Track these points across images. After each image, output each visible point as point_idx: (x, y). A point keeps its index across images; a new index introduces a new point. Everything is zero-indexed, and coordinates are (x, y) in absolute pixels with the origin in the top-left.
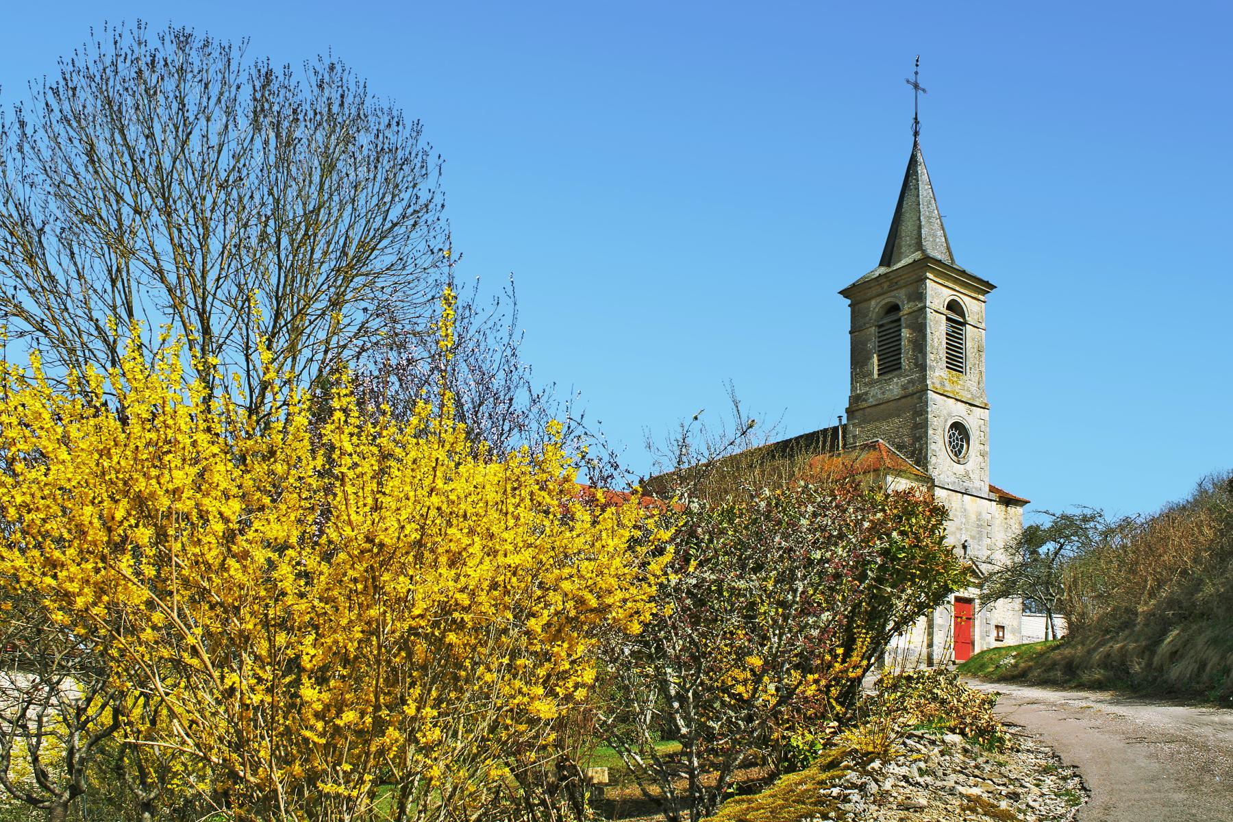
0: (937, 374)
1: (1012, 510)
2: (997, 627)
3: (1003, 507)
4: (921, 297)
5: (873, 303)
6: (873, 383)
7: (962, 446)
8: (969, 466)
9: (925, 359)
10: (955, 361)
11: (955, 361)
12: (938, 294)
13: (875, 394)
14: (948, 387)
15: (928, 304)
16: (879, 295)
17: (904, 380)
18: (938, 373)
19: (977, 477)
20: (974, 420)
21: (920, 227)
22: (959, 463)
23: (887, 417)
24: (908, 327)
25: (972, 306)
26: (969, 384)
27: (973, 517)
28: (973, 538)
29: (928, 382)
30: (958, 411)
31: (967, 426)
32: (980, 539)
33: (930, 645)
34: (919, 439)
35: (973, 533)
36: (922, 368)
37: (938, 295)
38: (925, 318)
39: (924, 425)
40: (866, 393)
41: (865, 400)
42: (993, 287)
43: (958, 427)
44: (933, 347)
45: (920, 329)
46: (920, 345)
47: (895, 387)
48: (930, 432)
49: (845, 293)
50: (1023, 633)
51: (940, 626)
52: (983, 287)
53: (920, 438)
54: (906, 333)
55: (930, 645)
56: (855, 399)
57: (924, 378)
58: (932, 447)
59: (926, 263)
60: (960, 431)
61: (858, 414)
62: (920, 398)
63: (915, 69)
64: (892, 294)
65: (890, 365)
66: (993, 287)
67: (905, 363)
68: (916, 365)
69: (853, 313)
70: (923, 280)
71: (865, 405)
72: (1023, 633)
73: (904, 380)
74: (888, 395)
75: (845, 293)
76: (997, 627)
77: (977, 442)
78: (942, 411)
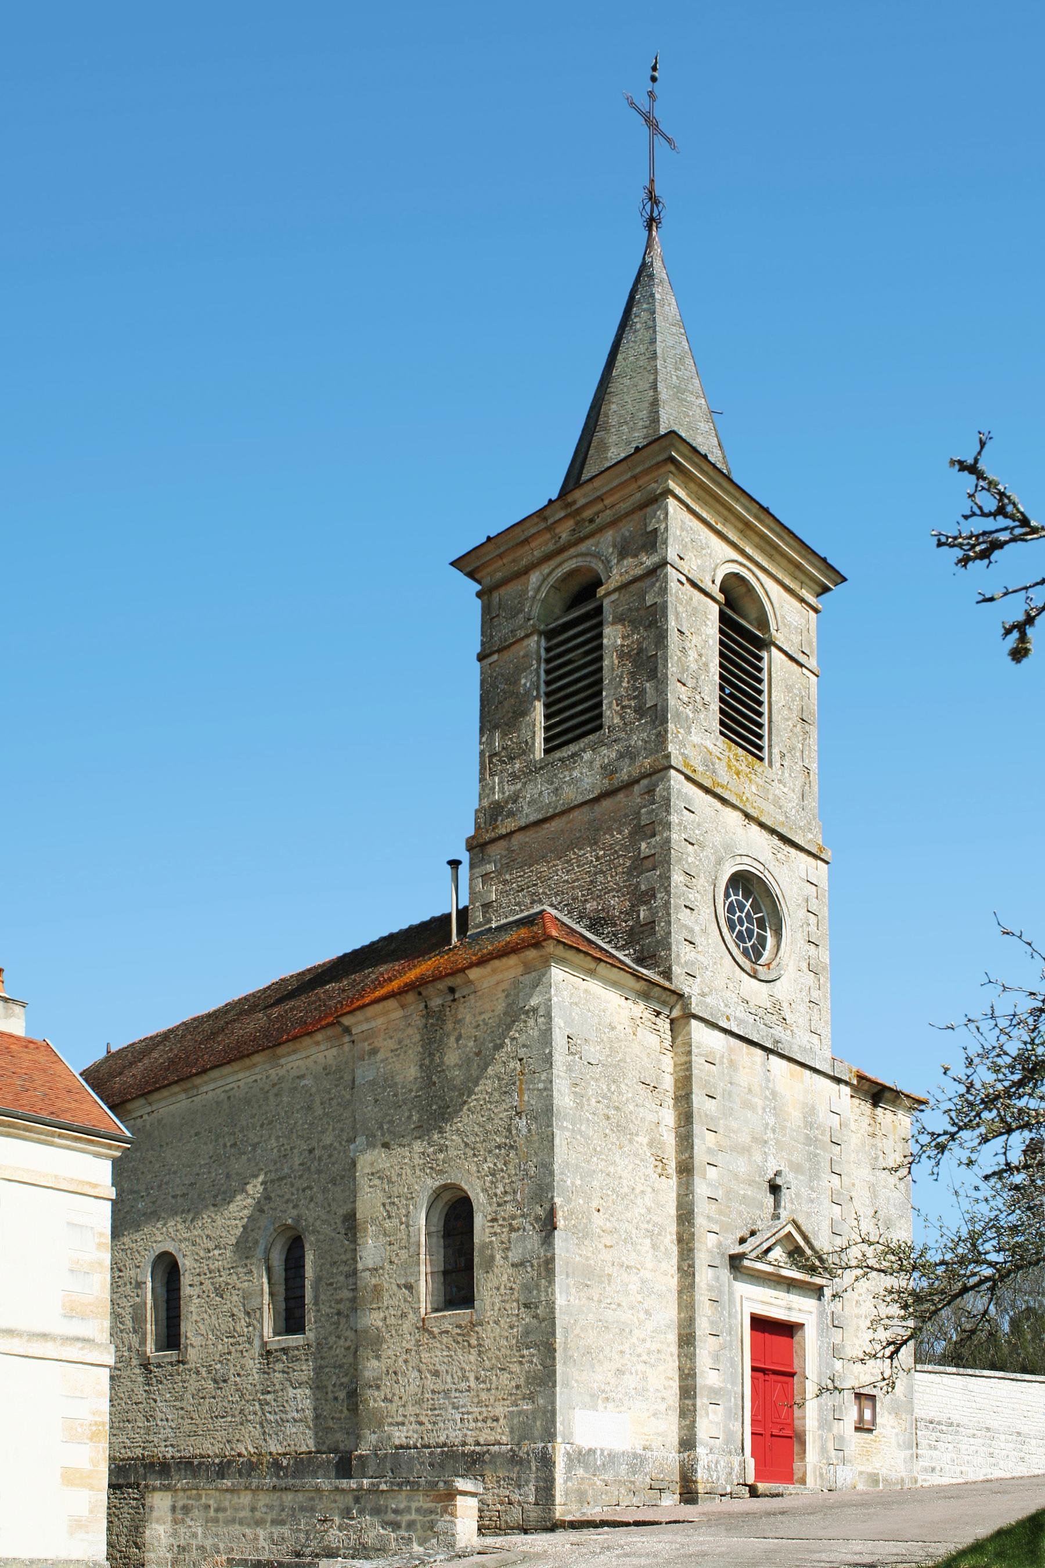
0: (695, 738)
1: (885, 1115)
2: (858, 1396)
3: (866, 1107)
4: (652, 540)
5: (534, 578)
6: (534, 770)
7: (762, 941)
8: (783, 989)
9: (661, 690)
10: (742, 718)
11: (742, 718)
12: (697, 550)
13: (537, 795)
14: (724, 776)
15: (672, 555)
16: (547, 558)
17: (609, 754)
18: (695, 734)
19: (802, 1021)
20: (791, 878)
21: (655, 403)
22: (754, 976)
23: (560, 850)
24: (619, 620)
25: (787, 615)
26: (786, 780)
27: (795, 1116)
28: (797, 1168)
29: (671, 748)
30: (756, 850)
31: (776, 890)
32: (814, 1176)
33: (688, 1443)
34: (647, 897)
35: (796, 1157)
36: (656, 716)
37: (701, 549)
38: (664, 591)
39: (660, 861)
40: (515, 798)
41: (511, 814)
42: (845, 579)
43: (745, 883)
44: (685, 669)
45: (651, 620)
46: (649, 664)
47: (586, 772)
48: (677, 878)
49: (468, 564)
50: (919, 1413)
51: (714, 1391)
52: (820, 576)
53: (650, 895)
54: (613, 636)
55: (688, 1443)
56: (491, 814)
57: (662, 738)
58: (681, 917)
59: (665, 453)
60: (752, 903)
61: (496, 851)
62: (650, 791)
63: (649, 86)
64: (582, 547)
65: (576, 717)
66: (845, 579)
67: (611, 714)
68: (640, 711)
69: (486, 610)
70: (657, 499)
71: (510, 825)
72: (919, 1413)
73: (609, 754)
74: (570, 795)
75: (468, 564)
76: (858, 1396)
77: (801, 938)
78: (708, 838)
